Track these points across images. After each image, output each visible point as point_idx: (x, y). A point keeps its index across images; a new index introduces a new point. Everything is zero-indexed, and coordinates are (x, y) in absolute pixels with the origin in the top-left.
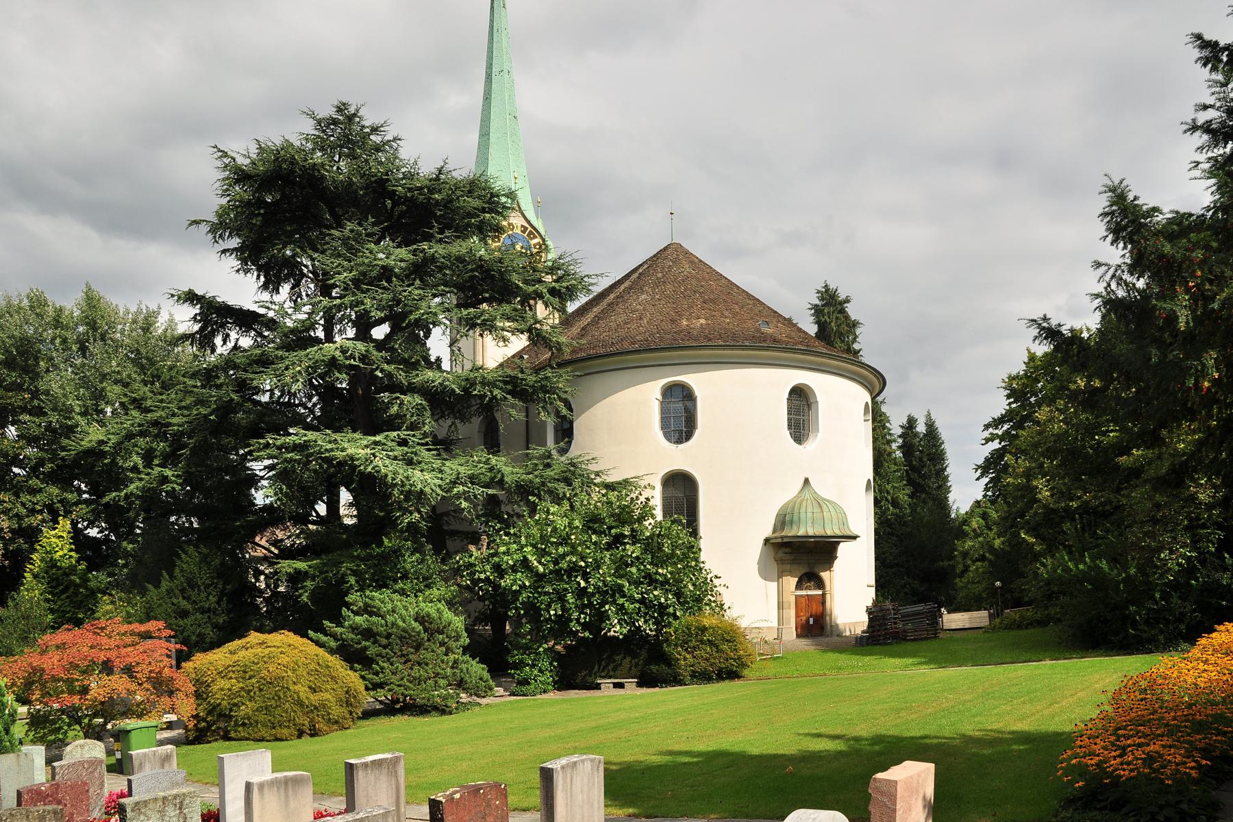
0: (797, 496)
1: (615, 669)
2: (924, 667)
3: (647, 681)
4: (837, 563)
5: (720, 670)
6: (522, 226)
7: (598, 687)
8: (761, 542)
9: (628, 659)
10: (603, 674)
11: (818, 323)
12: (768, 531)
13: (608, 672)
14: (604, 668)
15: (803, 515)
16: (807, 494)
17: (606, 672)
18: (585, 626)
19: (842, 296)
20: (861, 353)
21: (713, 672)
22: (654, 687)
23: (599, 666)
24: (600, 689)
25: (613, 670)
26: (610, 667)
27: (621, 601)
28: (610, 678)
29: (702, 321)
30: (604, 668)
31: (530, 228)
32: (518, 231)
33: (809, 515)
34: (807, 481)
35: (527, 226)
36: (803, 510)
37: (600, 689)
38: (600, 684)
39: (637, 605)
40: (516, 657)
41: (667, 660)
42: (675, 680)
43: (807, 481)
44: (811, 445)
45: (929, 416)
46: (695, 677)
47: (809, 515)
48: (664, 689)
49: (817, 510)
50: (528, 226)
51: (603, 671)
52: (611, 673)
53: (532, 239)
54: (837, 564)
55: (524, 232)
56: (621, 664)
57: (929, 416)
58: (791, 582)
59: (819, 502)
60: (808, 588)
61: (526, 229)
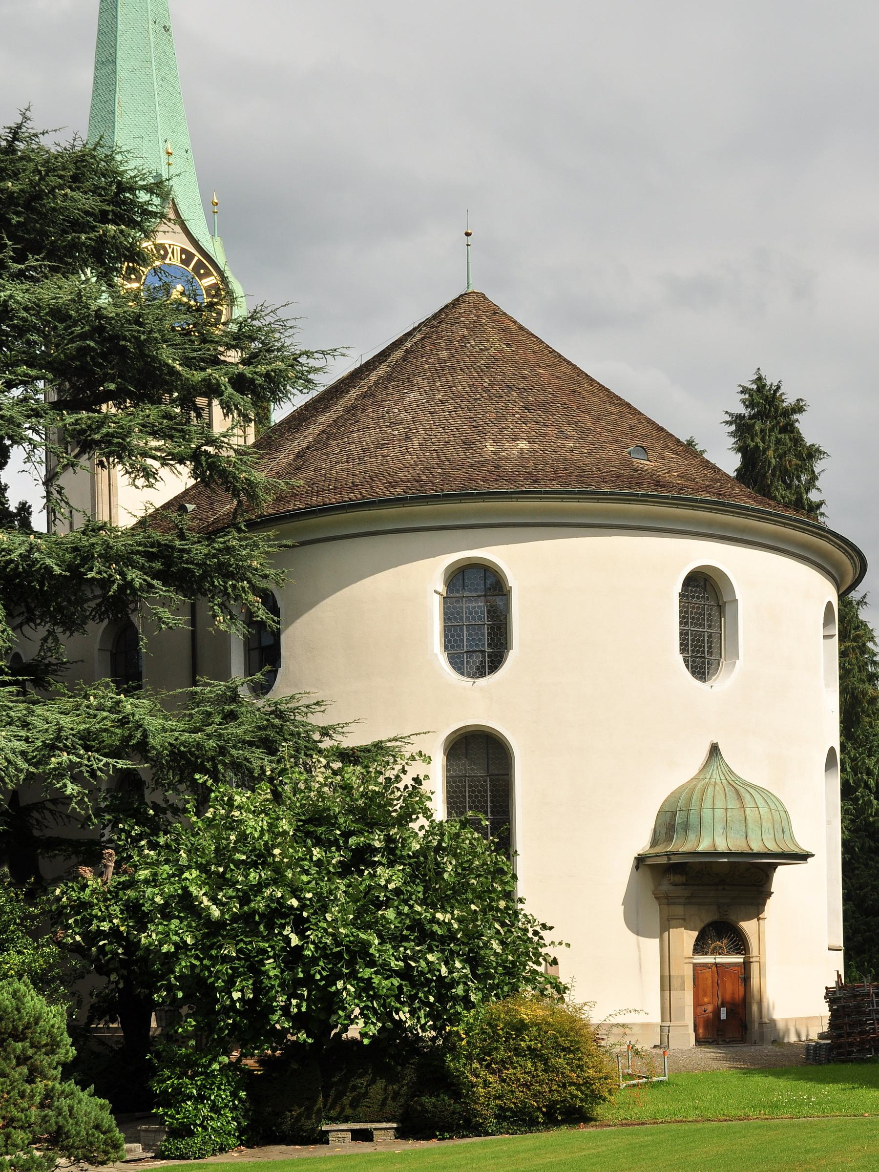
1: (354, 1104)
7: (322, 1139)
10: (333, 1113)
13: (343, 1109)
17: (338, 1109)
18: (300, 1021)
22: (428, 1138)
23: (326, 1097)
24: (327, 1142)
26: (346, 1100)
27: (366, 973)
28: (346, 1120)
37: (327, 1142)
38: (327, 1132)
39: (396, 982)
46: (505, 1118)
51: (332, 1107)
52: (348, 1111)
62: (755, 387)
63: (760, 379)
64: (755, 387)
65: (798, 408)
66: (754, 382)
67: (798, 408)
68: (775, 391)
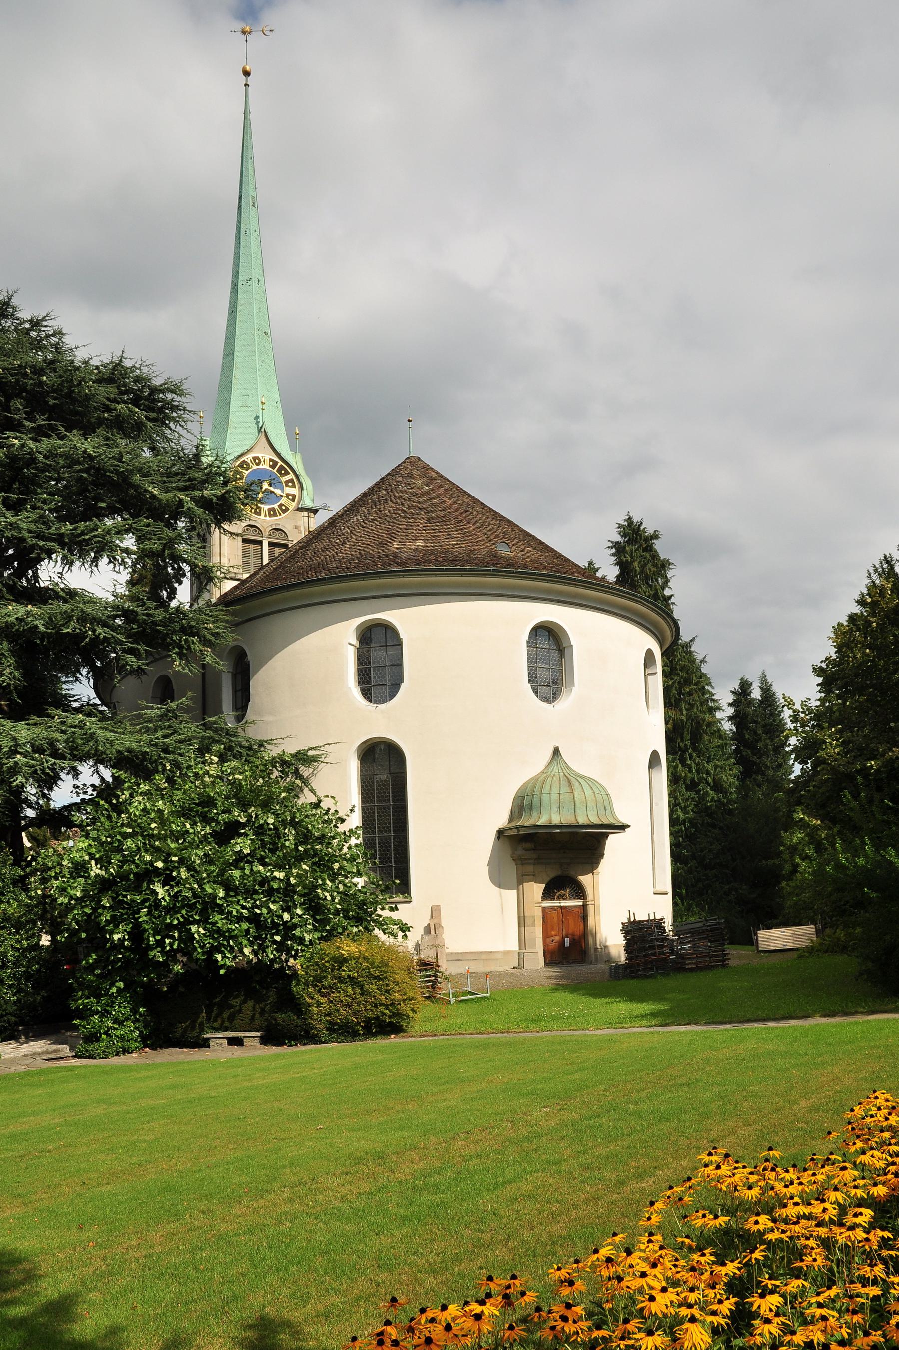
0: (542, 773)
1: (231, 1018)
2: (645, 1023)
3: (272, 1037)
4: (604, 863)
5: (368, 1021)
8: (493, 835)
9: (250, 1003)
10: (216, 1025)
11: (619, 563)
12: (502, 820)
13: (223, 1022)
14: (217, 1016)
15: (545, 797)
16: (556, 770)
17: (219, 1022)
19: (649, 527)
20: (672, 600)
21: (358, 1024)
23: (209, 1013)
24: (209, 1046)
25: (228, 1018)
28: (226, 1030)
30: (217, 1016)
33: (555, 797)
34: (556, 752)
36: (546, 791)
37: (209, 1046)
38: (208, 1039)
40: (81, 1001)
41: (294, 1004)
42: (308, 1037)
43: (556, 752)
44: (565, 703)
45: (763, 679)
47: (555, 797)
48: (294, 1049)
49: (565, 789)
51: (215, 1021)
52: (227, 1024)
54: (604, 865)
56: (240, 1011)
57: (763, 679)
58: (536, 890)
59: (570, 779)
60: (560, 898)
62: (626, 523)
63: (630, 518)
64: (626, 523)
65: (655, 536)
66: (625, 520)
67: (655, 536)
68: (640, 526)
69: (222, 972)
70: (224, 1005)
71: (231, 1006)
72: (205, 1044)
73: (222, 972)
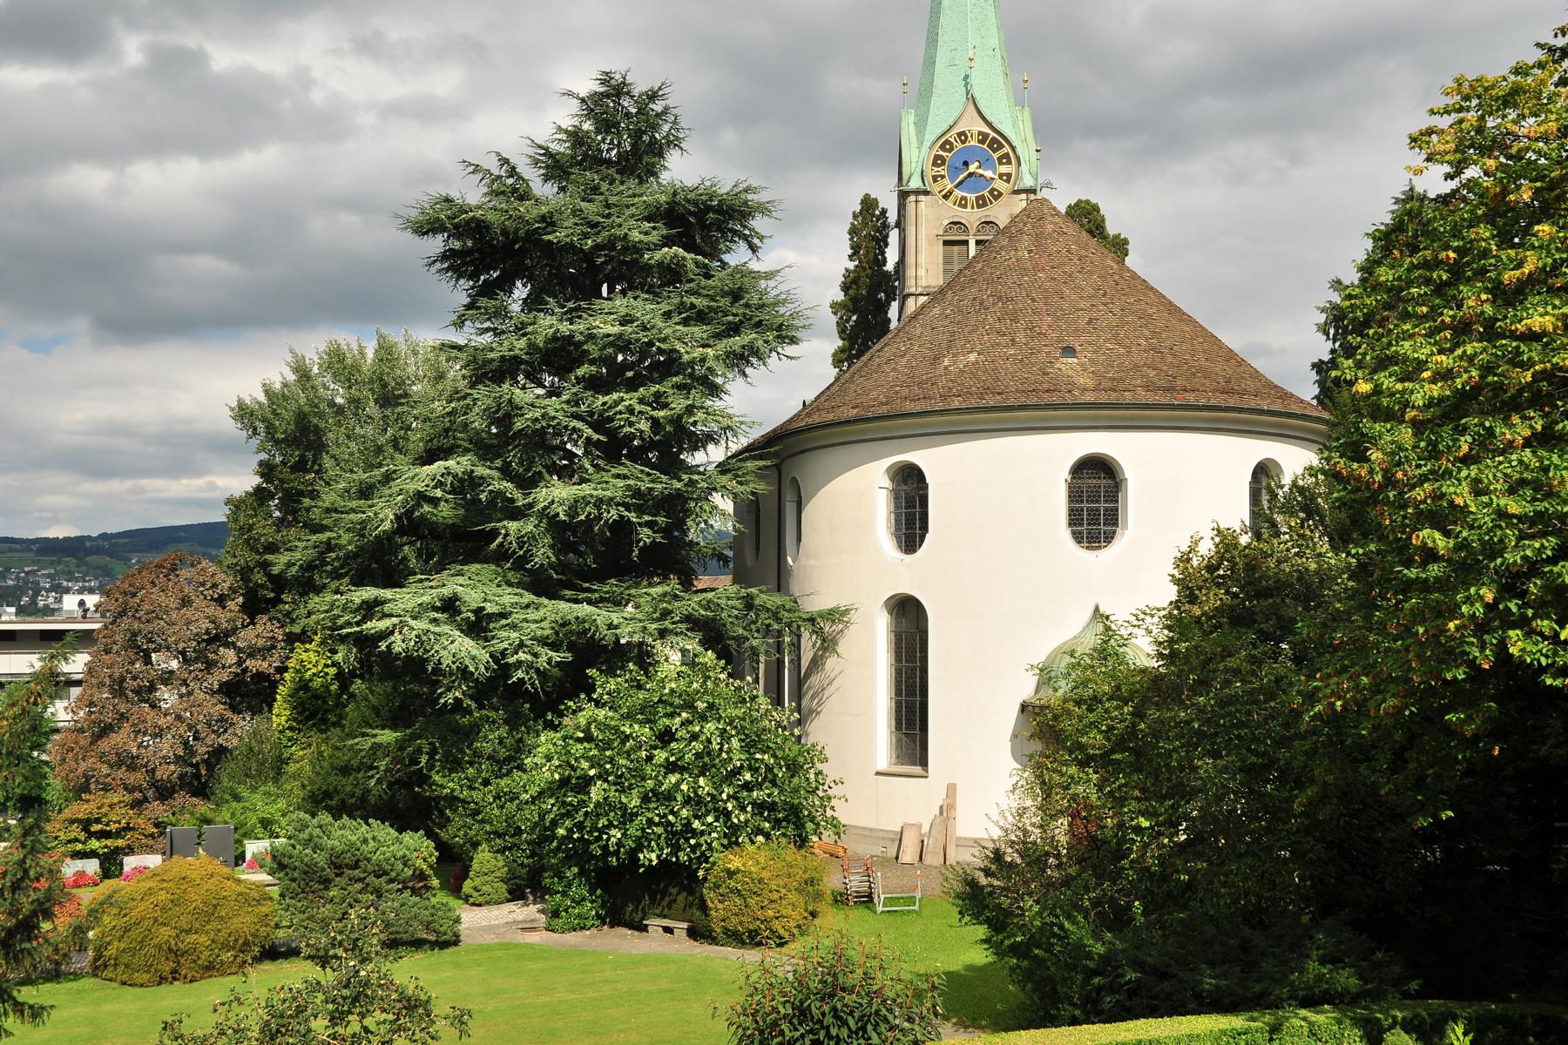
6: (980, 133)
29: (972, 357)
31: (992, 134)
32: (973, 143)
35: (987, 130)
50: (987, 130)
53: (994, 151)
55: (982, 142)
61: (985, 136)
69: (641, 870)
70: (664, 893)
71: (670, 894)
72: (644, 929)
73: (641, 870)
